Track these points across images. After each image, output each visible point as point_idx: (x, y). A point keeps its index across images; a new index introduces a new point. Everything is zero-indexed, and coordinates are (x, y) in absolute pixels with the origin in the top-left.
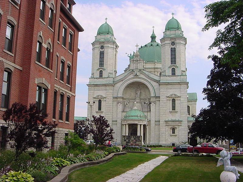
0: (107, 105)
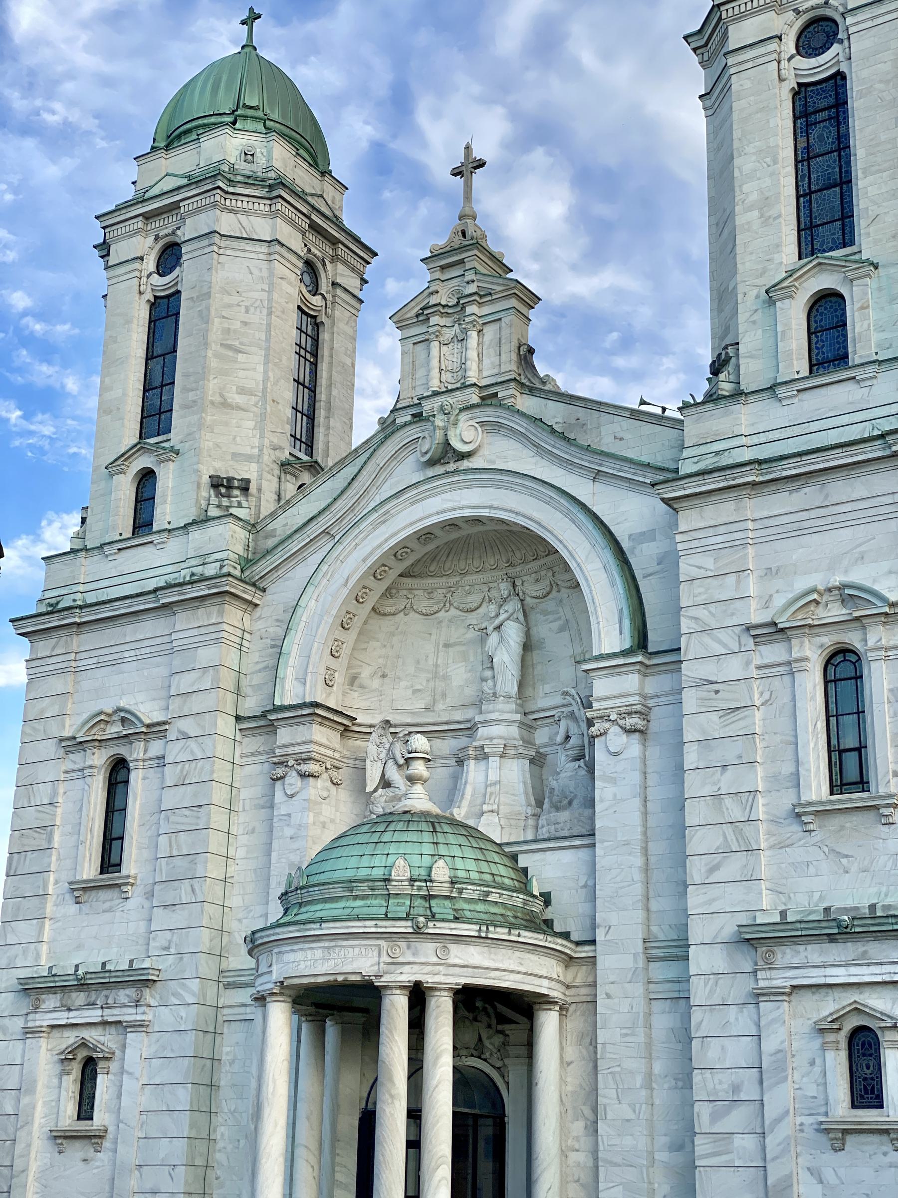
0: (171, 799)
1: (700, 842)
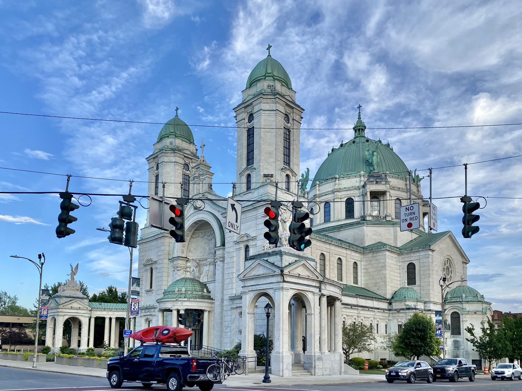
1: (227, 282)
